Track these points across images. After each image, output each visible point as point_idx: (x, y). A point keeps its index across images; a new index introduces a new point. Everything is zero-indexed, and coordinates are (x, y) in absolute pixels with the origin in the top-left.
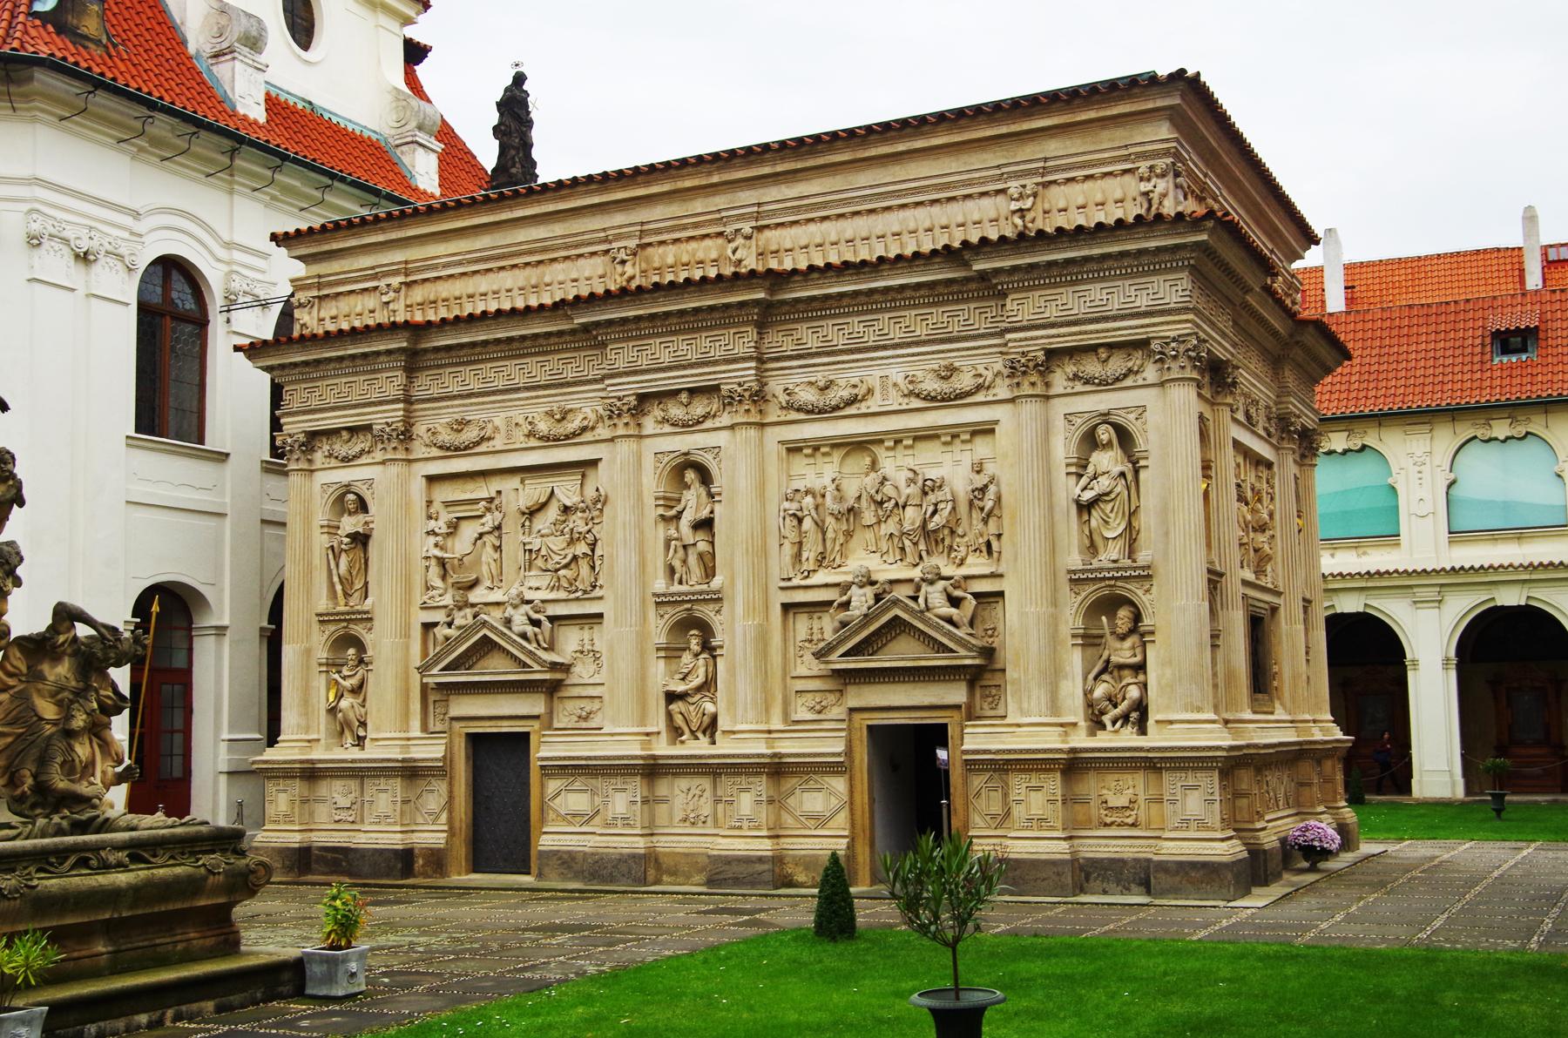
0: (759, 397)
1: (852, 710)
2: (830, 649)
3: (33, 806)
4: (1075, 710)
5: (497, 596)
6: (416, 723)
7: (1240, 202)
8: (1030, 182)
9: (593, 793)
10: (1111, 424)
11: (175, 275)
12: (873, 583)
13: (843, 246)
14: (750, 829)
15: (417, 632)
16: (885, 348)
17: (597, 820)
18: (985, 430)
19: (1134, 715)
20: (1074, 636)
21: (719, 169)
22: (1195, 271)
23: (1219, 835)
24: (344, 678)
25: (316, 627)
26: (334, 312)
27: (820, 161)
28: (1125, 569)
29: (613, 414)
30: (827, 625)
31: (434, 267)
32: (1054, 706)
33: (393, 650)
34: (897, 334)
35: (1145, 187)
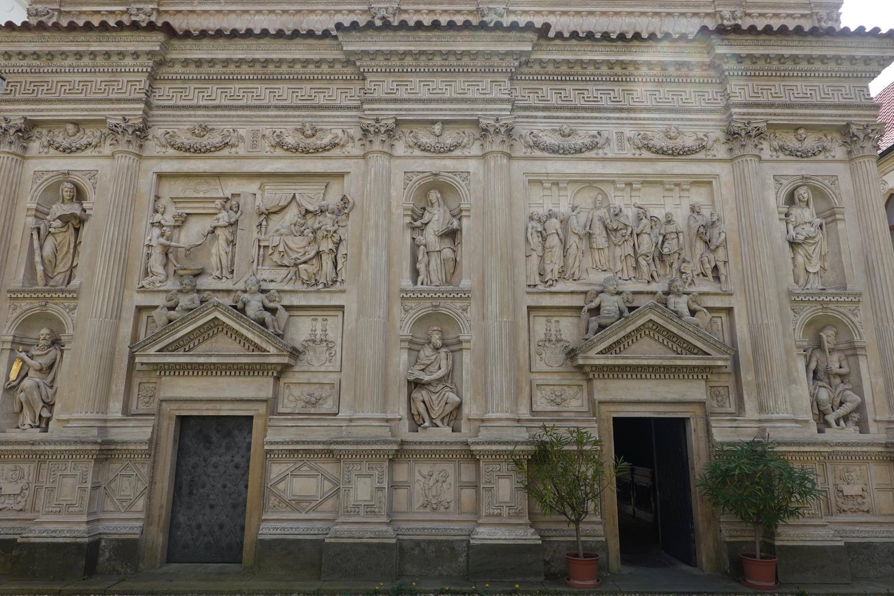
10: (810, 187)
14: (510, 516)
15: (129, 316)
18: (704, 182)
24: (32, 357)
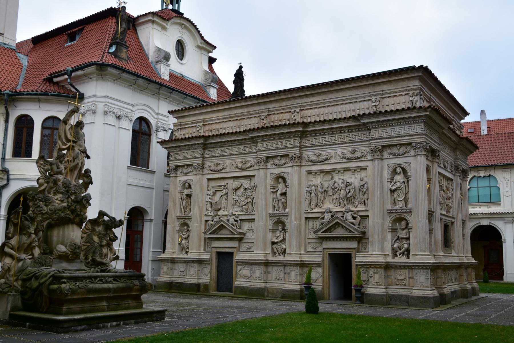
0: (300, 158)
1: (324, 249)
2: (318, 231)
3: (91, 265)
4: (389, 251)
5: (226, 213)
6: (202, 248)
7: (443, 103)
8: (378, 97)
9: (251, 270)
11: (143, 122)
12: (331, 212)
13: (324, 115)
15: (203, 222)
16: (336, 144)
17: (251, 278)
18: (364, 168)
19: (406, 253)
20: (389, 229)
21: (290, 93)
22: (426, 123)
23: (430, 289)
25: (176, 220)
26: (184, 133)
27: (319, 91)
28: (404, 210)
29: (259, 162)
30: (318, 223)
31: (212, 120)
32: (382, 249)
33: (197, 227)
34: (339, 141)
35: (411, 99)
